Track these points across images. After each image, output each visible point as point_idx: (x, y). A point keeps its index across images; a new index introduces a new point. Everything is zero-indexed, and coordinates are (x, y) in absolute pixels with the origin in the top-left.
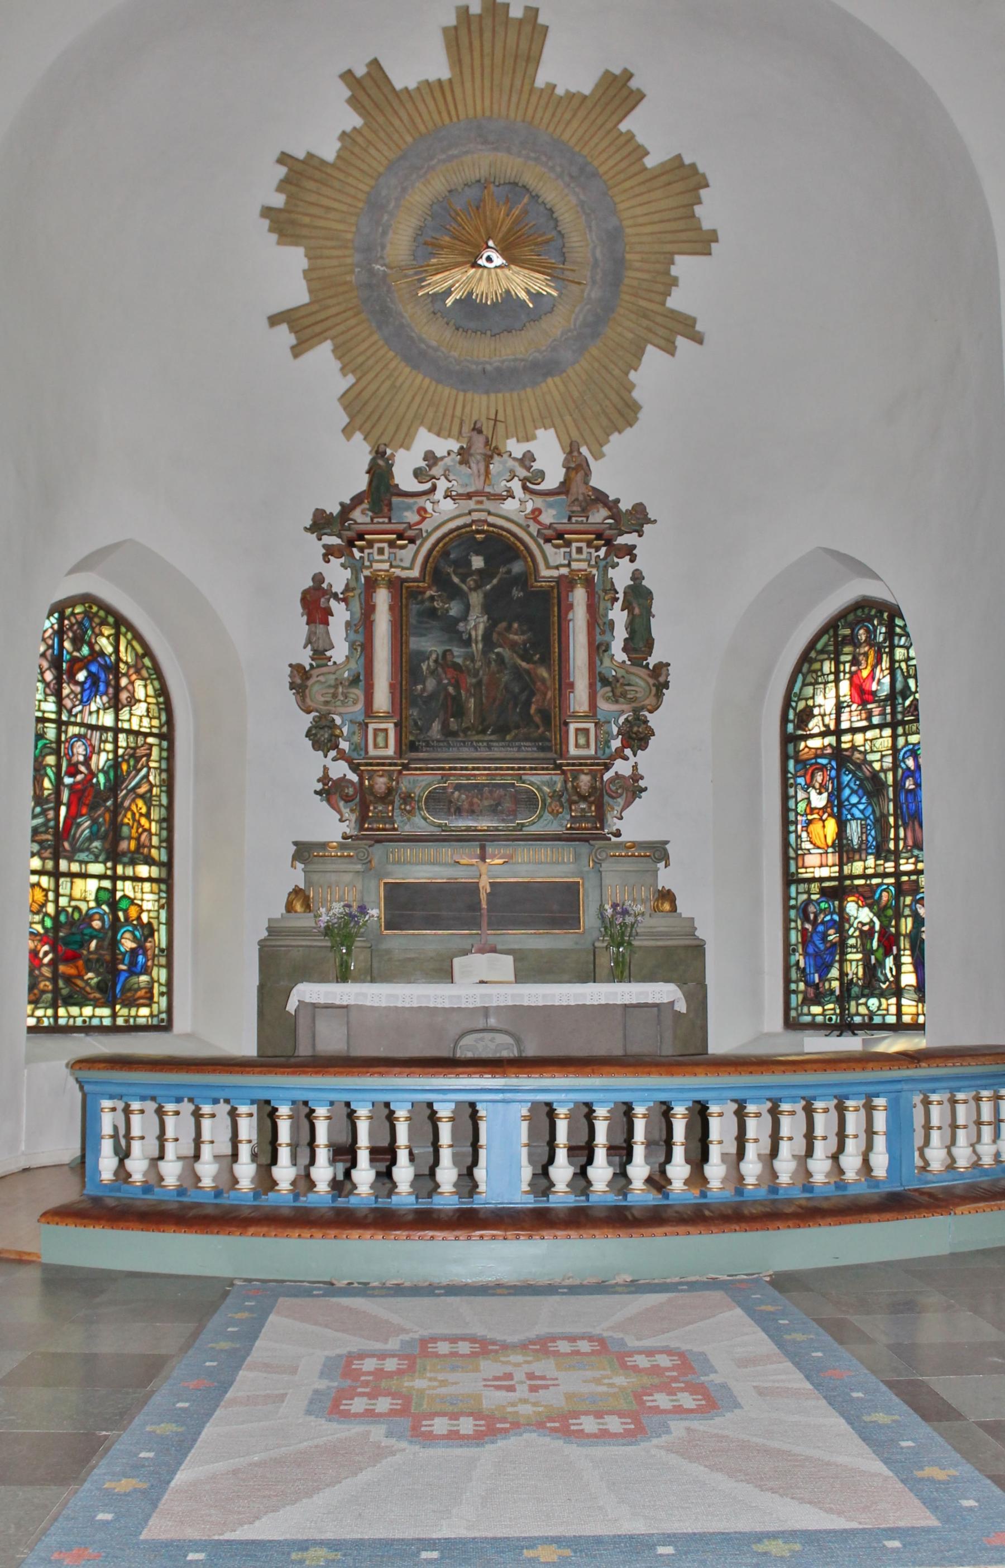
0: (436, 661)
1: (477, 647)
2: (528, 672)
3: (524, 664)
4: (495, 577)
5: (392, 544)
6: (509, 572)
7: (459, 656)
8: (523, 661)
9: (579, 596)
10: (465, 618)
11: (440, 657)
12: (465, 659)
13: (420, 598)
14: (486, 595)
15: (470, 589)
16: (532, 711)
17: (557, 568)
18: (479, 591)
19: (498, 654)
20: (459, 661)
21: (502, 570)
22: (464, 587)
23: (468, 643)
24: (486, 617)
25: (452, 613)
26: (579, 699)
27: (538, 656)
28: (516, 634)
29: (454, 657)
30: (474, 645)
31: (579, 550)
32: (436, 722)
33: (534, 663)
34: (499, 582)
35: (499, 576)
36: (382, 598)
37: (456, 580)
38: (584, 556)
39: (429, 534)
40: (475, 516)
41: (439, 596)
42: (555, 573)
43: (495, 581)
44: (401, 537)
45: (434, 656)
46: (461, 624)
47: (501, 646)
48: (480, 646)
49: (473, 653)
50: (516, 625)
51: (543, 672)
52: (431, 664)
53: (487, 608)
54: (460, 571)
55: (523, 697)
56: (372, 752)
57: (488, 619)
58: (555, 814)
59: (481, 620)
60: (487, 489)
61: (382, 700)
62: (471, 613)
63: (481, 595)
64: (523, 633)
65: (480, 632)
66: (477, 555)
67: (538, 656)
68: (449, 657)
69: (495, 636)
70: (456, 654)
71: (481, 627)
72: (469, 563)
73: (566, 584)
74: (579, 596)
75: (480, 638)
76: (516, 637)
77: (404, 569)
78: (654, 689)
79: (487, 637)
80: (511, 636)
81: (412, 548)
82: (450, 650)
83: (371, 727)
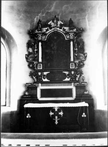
5: (42, 35)
9: (72, 43)
10: (53, 47)
17: (68, 38)
26: (72, 59)
31: (71, 35)
36: (40, 44)
38: (72, 36)
39: (48, 33)
40: (55, 30)
42: (68, 39)
44: (43, 34)
56: (38, 69)
58: (68, 78)
60: (57, 26)
61: (40, 60)
73: (70, 40)
74: (72, 43)
77: (44, 39)
78: (84, 58)
81: (45, 36)
83: (38, 65)
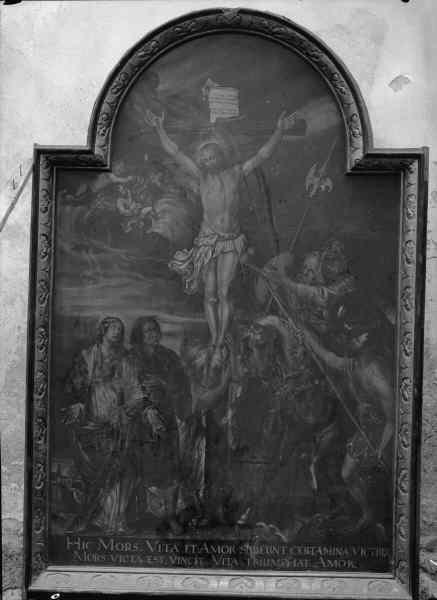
0: (116, 346)
1: (219, 313)
2: (338, 376)
3: (329, 357)
6: (300, 128)
7: (170, 334)
8: (327, 347)
11: (127, 337)
12: (186, 342)
13: (82, 189)
15: (205, 171)
16: (345, 473)
20: (174, 345)
21: (285, 122)
22: (190, 165)
23: (196, 303)
24: (239, 242)
25: (160, 228)
27: (363, 338)
28: (314, 283)
30: (209, 309)
32: (115, 493)
33: (355, 354)
34: (274, 151)
35: (273, 141)
37: (170, 146)
41: (129, 185)
43: (264, 151)
45: (112, 333)
46: (180, 256)
47: (274, 311)
48: (225, 311)
49: (207, 325)
50: (312, 261)
51: (373, 376)
52: (105, 349)
54: (181, 124)
55: (327, 435)
57: (247, 245)
59: (229, 245)
62: (206, 230)
63: (230, 185)
64: (329, 282)
66: (223, 84)
67: (363, 338)
68: (149, 338)
69: (261, 288)
70: (165, 328)
71: (228, 264)
72: (203, 107)
75: (224, 291)
76: (313, 290)
79: (242, 288)
80: (300, 286)
82: (152, 319)
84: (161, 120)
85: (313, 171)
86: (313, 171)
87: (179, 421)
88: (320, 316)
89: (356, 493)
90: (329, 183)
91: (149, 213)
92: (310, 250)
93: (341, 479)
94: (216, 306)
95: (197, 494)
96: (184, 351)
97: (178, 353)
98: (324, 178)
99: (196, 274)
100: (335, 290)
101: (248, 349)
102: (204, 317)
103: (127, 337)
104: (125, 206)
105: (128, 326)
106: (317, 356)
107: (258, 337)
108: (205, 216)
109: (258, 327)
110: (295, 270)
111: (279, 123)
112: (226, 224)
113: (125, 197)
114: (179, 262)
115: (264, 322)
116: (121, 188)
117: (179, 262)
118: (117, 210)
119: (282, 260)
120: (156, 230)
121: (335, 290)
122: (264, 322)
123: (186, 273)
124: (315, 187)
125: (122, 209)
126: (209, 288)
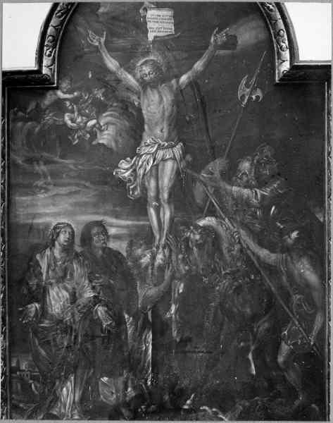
0: (67, 249)
2: (272, 270)
3: (264, 253)
4: (199, 56)
6: (231, 42)
7: (117, 237)
8: (261, 244)
11: (77, 240)
12: (131, 244)
13: (32, 106)
14: (180, 97)
18: (163, 88)
19: (205, 228)
20: (120, 246)
23: (140, 207)
24: (178, 150)
25: (105, 138)
27: (294, 235)
29: (108, 237)
30: (152, 211)
33: (286, 250)
37: (112, 64)
41: (75, 101)
43: (199, 65)
45: (63, 238)
46: (124, 165)
47: (212, 213)
49: (150, 227)
50: (246, 165)
52: (57, 252)
53: (179, 126)
54: (120, 42)
63: (168, 98)
64: (262, 183)
65: (166, 180)
67: (294, 235)
68: (97, 241)
69: (199, 191)
70: (112, 231)
76: (246, 192)
79: (181, 192)
80: (235, 189)
82: (100, 224)
84: (103, 40)
85: (244, 82)
86: (244, 82)
87: (126, 316)
88: (254, 216)
89: (292, 377)
90: (259, 93)
91: (94, 126)
92: (242, 156)
93: (277, 363)
94: (158, 210)
95: (146, 384)
96: (130, 252)
97: (125, 254)
98: (254, 89)
99: (139, 181)
100: (267, 192)
101: (188, 249)
102: (148, 220)
103: (77, 240)
104: (73, 120)
105: (78, 230)
106: (253, 254)
107: (198, 237)
108: (146, 127)
109: (197, 227)
110: (230, 174)
111: (212, 39)
112: (166, 134)
113: (73, 112)
114: (124, 169)
115: (202, 223)
116: (68, 103)
117: (124, 169)
118: (65, 124)
119: (217, 166)
120: (101, 142)
121: (267, 192)
122: (202, 223)
123: (130, 180)
124: (247, 97)
125: (69, 123)
126: (152, 194)
